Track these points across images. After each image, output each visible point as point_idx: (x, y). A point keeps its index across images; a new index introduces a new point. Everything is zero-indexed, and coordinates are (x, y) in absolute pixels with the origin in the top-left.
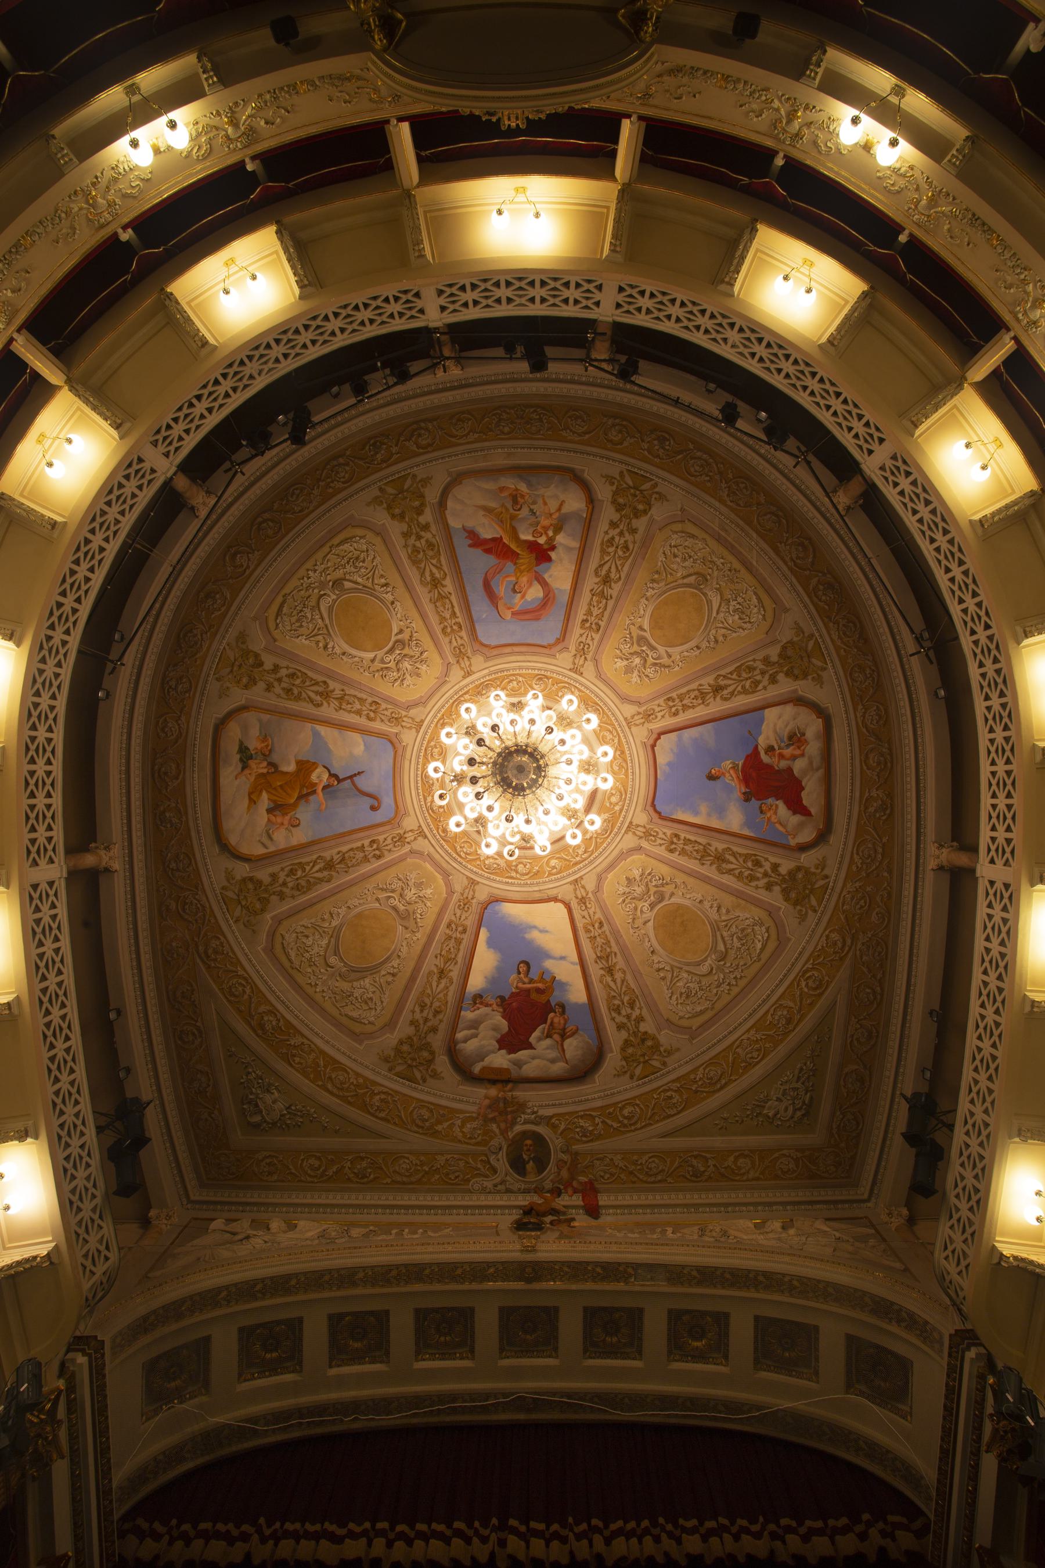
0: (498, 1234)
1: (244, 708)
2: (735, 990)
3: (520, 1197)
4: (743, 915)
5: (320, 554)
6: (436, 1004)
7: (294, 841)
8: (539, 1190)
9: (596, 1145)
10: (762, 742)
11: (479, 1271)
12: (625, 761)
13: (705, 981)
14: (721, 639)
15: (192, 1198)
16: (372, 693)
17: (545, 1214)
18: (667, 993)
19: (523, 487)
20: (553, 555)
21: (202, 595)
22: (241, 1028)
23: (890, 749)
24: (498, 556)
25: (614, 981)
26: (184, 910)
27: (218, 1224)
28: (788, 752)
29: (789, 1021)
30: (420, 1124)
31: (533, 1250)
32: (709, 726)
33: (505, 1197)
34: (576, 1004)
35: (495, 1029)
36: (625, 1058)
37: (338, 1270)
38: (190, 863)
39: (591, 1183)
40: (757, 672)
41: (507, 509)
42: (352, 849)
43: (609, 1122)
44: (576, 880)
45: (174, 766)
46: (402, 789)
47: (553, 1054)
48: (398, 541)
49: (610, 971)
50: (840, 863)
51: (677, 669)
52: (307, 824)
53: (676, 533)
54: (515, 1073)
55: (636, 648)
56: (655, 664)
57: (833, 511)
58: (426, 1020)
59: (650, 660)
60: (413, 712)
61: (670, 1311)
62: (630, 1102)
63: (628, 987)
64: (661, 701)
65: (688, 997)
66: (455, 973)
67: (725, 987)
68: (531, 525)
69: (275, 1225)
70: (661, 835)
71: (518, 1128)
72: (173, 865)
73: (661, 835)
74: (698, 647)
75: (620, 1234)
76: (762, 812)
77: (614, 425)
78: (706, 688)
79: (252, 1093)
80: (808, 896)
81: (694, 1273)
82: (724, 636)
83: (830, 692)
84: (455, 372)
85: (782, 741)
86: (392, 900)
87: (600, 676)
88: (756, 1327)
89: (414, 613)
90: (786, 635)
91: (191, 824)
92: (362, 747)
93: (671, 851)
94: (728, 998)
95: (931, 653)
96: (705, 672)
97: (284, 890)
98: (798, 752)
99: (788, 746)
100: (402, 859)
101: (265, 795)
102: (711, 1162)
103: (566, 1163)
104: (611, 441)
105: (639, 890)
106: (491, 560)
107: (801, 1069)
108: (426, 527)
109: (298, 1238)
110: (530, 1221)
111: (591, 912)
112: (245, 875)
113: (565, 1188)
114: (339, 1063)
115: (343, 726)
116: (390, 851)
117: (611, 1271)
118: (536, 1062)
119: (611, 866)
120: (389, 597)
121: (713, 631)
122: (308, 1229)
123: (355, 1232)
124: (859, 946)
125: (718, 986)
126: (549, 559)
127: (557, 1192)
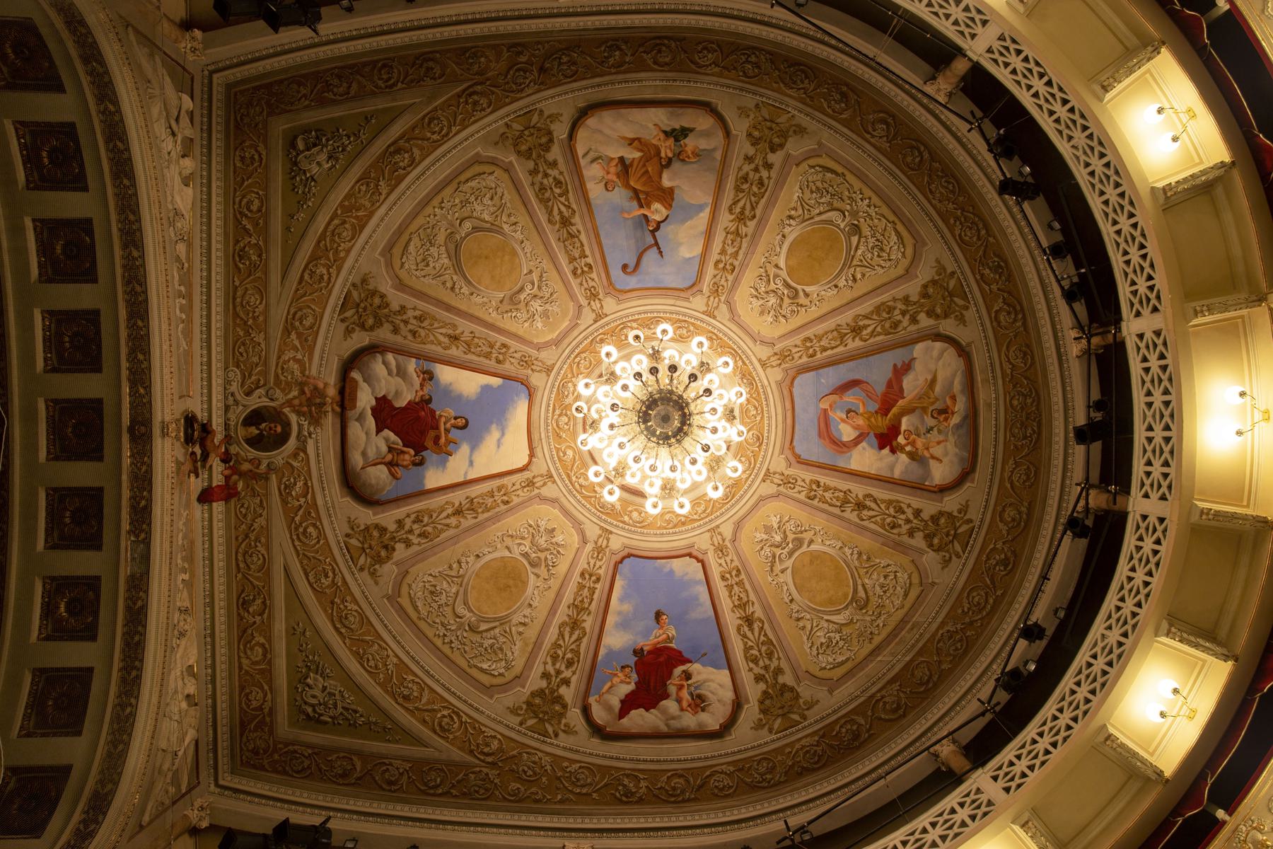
0: (180, 397)
1: (727, 133)
2: (439, 642)
3: (221, 421)
4: (517, 649)
5: (885, 210)
6: (422, 332)
7: (590, 186)
8: (228, 439)
9: (276, 498)
10: (695, 667)
11: (141, 378)
12: (675, 527)
13: (448, 610)
14: (801, 624)
15: (215, 76)
16: (743, 265)
17: (203, 446)
18: (435, 571)
19: (955, 420)
20: (886, 451)
21: (844, 89)
22: (396, 130)
23: (689, 800)
24: (885, 395)
25: (448, 517)
26: (518, 70)
27: (187, 103)
28: (685, 694)
29: (406, 698)
30: (297, 316)
31: (164, 434)
32: (712, 613)
33: (221, 405)
34: (424, 477)
35: (398, 394)
36: (367, 528)
37: (140, 229)
38: (566, 77)
39: (237, 494)
40: (767, 662)
41: (933, 403)
42: (582, 245)
43: (301, 513)
44: (551, 476)
45: (667, 60)
46: (645, 297)
47: (372, 454)
48: (899, 291)
49: (458, 512)
50: (571, 750)
51: (770, 579)
52: (608, 199)
53: (910, 577)
54: (351, 414)
55: (791, 537)
56: (774, 557)
57: (934, 739)
58: (406, 322)
59: (778, 551)
60: (723, 307)
61: (98, 578)
62: (321, 534)
63: (441, 531)
64: (736, 563)
65: (432, 593)
66: (455, 352)
67: (442, 631)
68: (917, 428)
69: (188, 164)
70: (598, 564)
71: (293, 418)
72: (565, 59)
73: (598, 564)
74: (792, 601)
75: (181, 524)
76: (623, 667)
77: (1020, 513)
78: (750, 610)
79: (328, 140)
80: (537, 717)
81: (140, 603)
82: (804, 628)
83: (748, 736)
84: (1075, 349)
85: (696, 688)
86: (530, 287)
87: (762, 499)
88: (80, 669)
89: (826, 308)
90: (806, 691)
91: (607, 78)
92: (688, 256)
93: (582, 574)
94: (430, 635)
95: (788, 842)
96: (766, 608)
97: (540, 175)
98: (685, 704)
99: (691, 694)
100: (572, 297)
101: (638, 155)
102: (258, 619)
103: (258, 468)
104: (1004, 510)
105: (542, 542)
106: (880, 388)
107: (356, 712)
108: (914, 320)
109: (173, 185)
110: (195, 431)
111: (519, 492)
112: (555, 134)
113: (230, 468)
114: (361, 232)
115: (709, 235)
116: (581, 284)
117: (142, 515)
118: (363, 436)
119: (566, 513)
120: (842, 283)
121: (808, 616)
122: (184, 198)
123: (181, 248)
124: (485, 770)
125: (442, 624)
126: (881, 447)
127: (226, 459)
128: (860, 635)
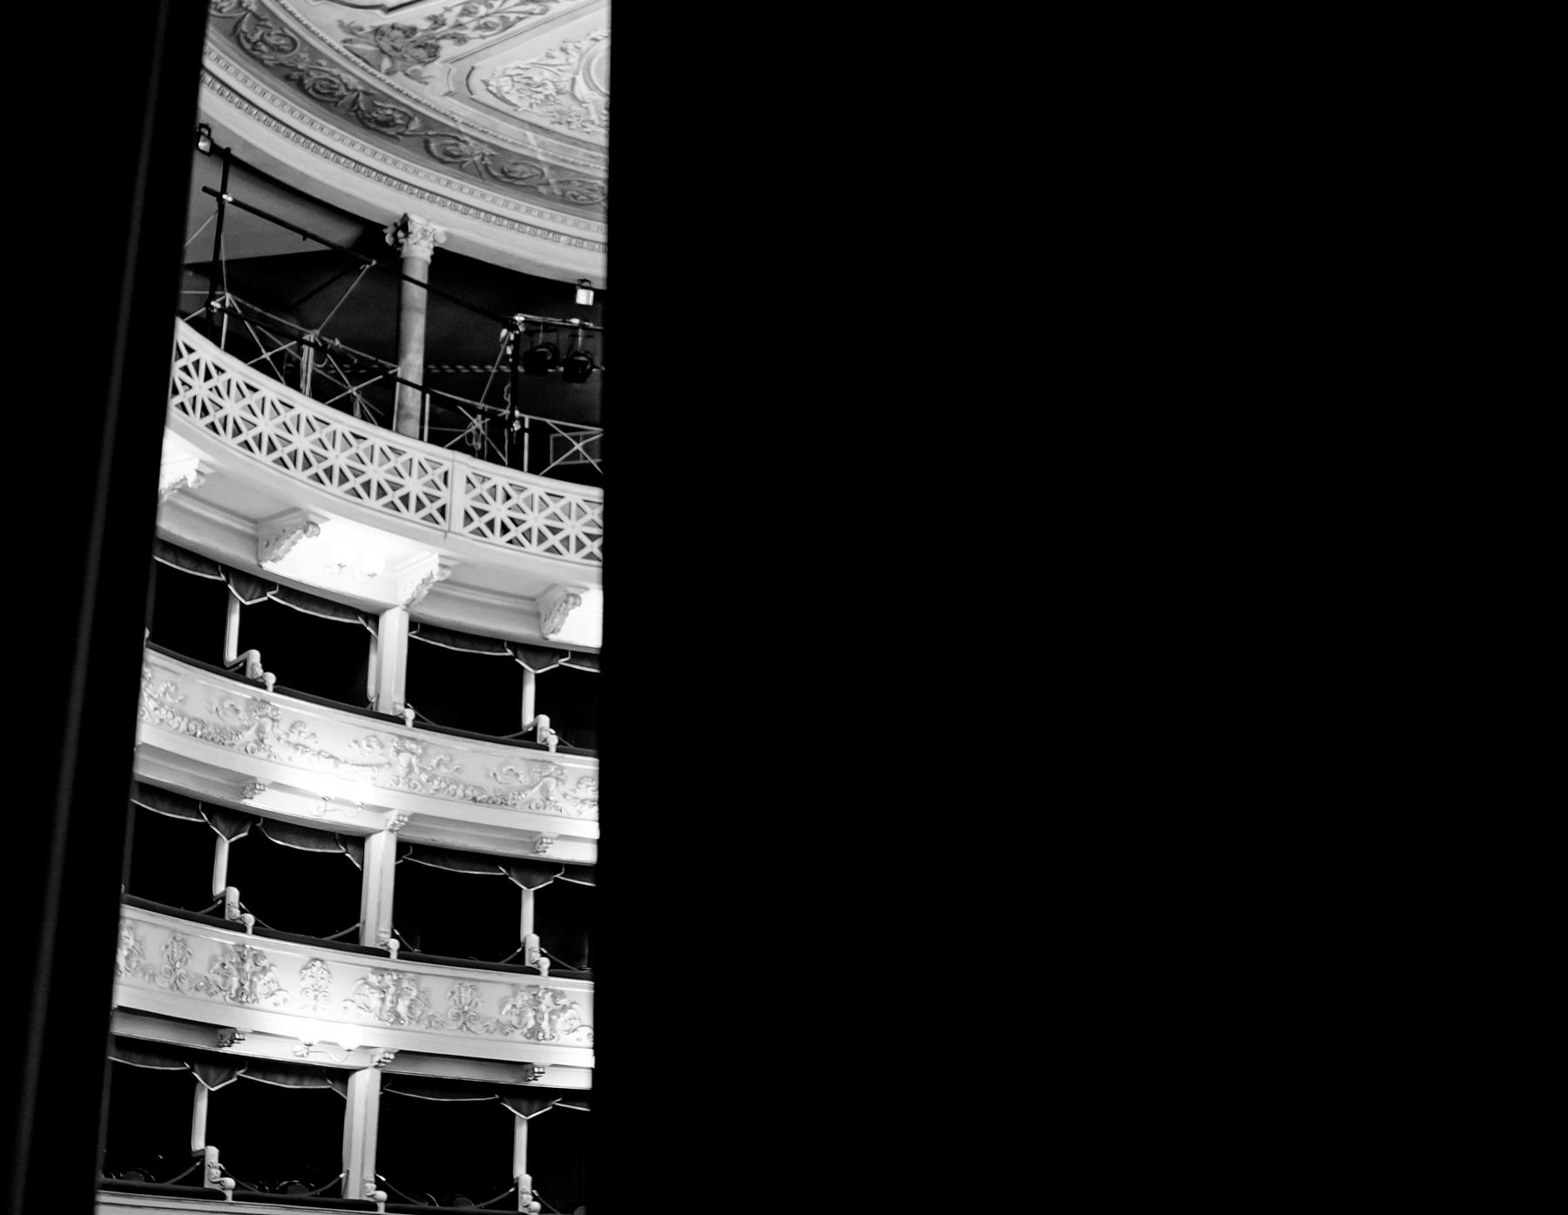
128: (561, 113)
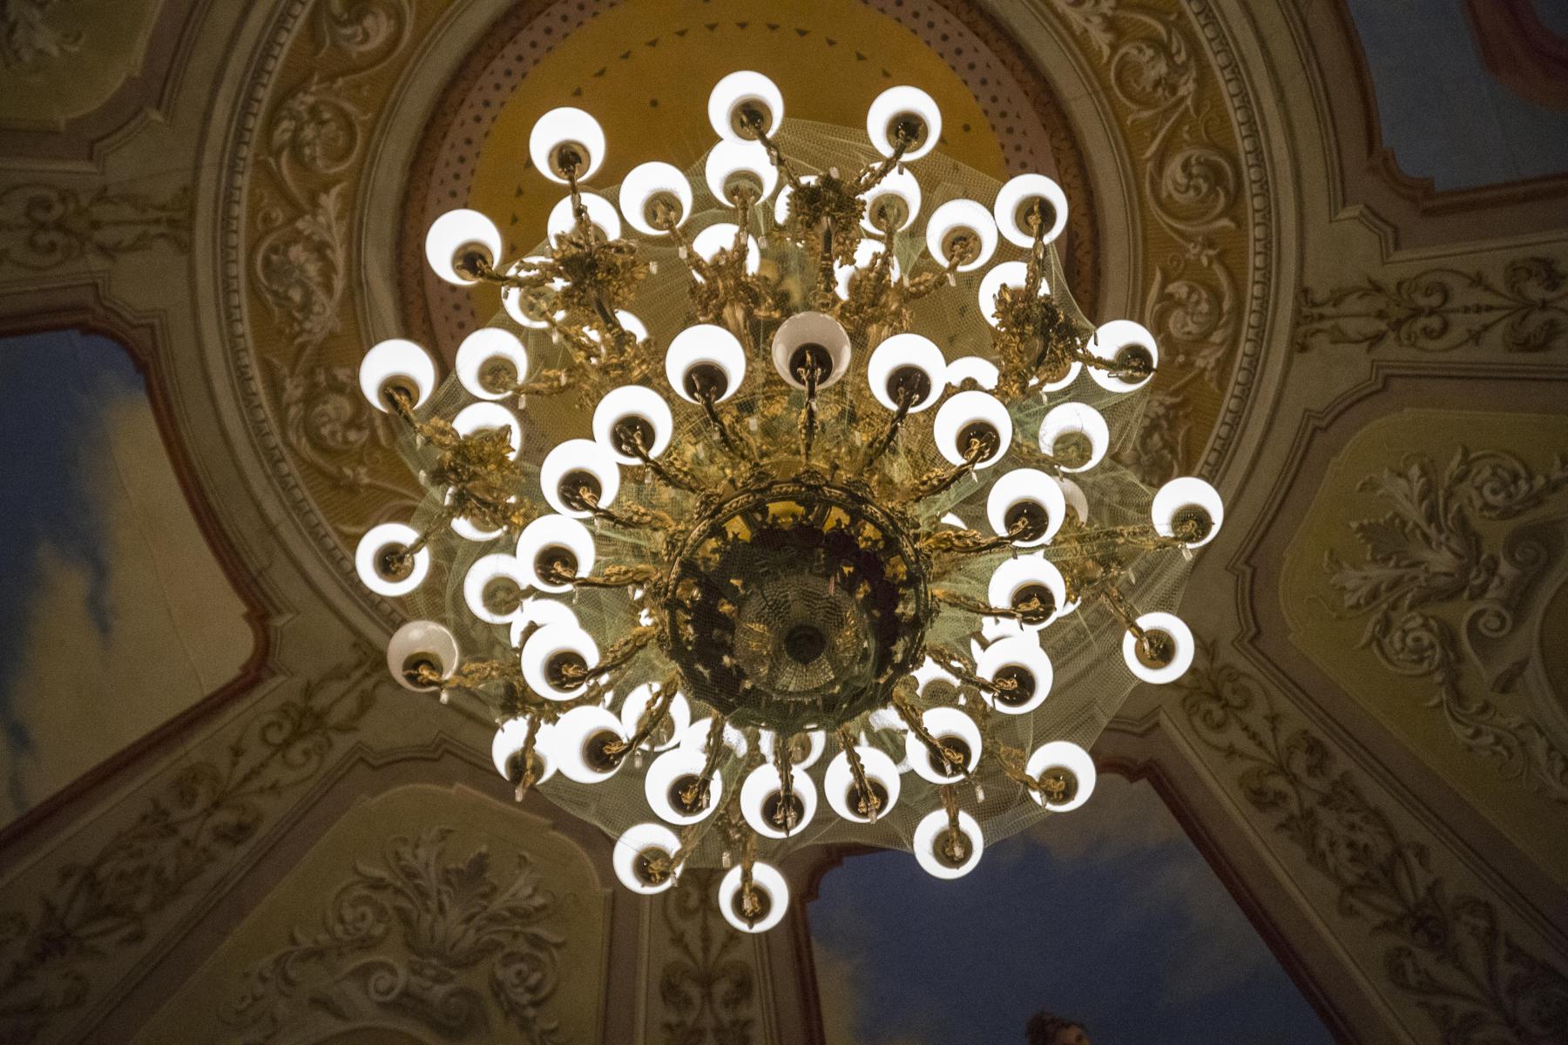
32: (1258, 950)
51: (1462, 733)
55: (1495, 534)
56: (1449, 639)
59: (1460, 614)
